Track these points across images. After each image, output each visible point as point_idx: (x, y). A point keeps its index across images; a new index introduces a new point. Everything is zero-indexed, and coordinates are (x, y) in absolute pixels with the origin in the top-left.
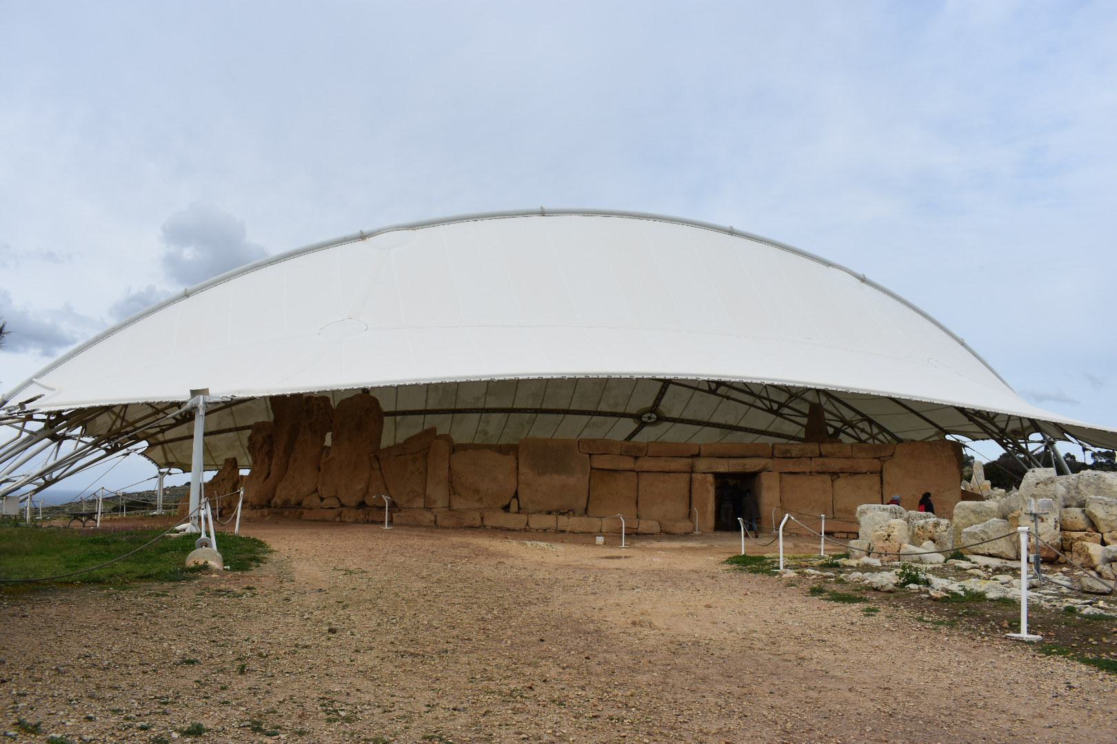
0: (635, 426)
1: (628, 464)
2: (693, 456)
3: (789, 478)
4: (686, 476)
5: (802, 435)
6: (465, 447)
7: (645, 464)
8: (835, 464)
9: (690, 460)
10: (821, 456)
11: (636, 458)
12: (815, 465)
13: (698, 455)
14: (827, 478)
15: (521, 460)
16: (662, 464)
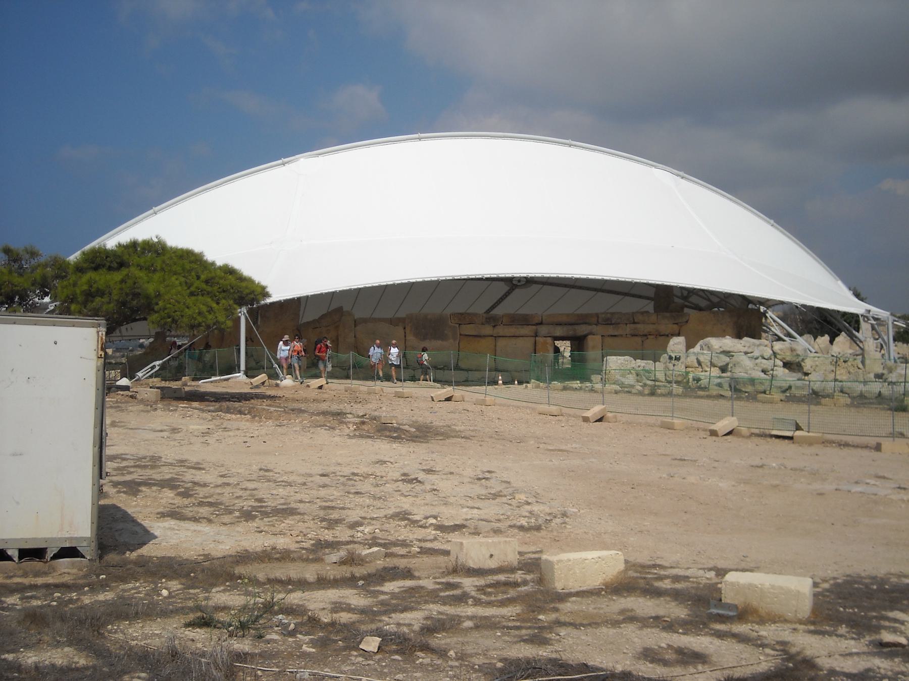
0: (506, 288)
1: (488, 330)
2: (537, 324)
3: (609, 341)
4: (533, 339)
5: (653, 296)
6: (365, 321)
7: (500, 330)
8: (642, 328)
9: (534, 327)
10: (634, 323)
11: (494, 326)
12: (629, 329)
13: (541, 323)
14: (639, 339)
15: (408, 331)
16: (512, 330)
